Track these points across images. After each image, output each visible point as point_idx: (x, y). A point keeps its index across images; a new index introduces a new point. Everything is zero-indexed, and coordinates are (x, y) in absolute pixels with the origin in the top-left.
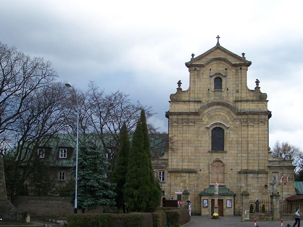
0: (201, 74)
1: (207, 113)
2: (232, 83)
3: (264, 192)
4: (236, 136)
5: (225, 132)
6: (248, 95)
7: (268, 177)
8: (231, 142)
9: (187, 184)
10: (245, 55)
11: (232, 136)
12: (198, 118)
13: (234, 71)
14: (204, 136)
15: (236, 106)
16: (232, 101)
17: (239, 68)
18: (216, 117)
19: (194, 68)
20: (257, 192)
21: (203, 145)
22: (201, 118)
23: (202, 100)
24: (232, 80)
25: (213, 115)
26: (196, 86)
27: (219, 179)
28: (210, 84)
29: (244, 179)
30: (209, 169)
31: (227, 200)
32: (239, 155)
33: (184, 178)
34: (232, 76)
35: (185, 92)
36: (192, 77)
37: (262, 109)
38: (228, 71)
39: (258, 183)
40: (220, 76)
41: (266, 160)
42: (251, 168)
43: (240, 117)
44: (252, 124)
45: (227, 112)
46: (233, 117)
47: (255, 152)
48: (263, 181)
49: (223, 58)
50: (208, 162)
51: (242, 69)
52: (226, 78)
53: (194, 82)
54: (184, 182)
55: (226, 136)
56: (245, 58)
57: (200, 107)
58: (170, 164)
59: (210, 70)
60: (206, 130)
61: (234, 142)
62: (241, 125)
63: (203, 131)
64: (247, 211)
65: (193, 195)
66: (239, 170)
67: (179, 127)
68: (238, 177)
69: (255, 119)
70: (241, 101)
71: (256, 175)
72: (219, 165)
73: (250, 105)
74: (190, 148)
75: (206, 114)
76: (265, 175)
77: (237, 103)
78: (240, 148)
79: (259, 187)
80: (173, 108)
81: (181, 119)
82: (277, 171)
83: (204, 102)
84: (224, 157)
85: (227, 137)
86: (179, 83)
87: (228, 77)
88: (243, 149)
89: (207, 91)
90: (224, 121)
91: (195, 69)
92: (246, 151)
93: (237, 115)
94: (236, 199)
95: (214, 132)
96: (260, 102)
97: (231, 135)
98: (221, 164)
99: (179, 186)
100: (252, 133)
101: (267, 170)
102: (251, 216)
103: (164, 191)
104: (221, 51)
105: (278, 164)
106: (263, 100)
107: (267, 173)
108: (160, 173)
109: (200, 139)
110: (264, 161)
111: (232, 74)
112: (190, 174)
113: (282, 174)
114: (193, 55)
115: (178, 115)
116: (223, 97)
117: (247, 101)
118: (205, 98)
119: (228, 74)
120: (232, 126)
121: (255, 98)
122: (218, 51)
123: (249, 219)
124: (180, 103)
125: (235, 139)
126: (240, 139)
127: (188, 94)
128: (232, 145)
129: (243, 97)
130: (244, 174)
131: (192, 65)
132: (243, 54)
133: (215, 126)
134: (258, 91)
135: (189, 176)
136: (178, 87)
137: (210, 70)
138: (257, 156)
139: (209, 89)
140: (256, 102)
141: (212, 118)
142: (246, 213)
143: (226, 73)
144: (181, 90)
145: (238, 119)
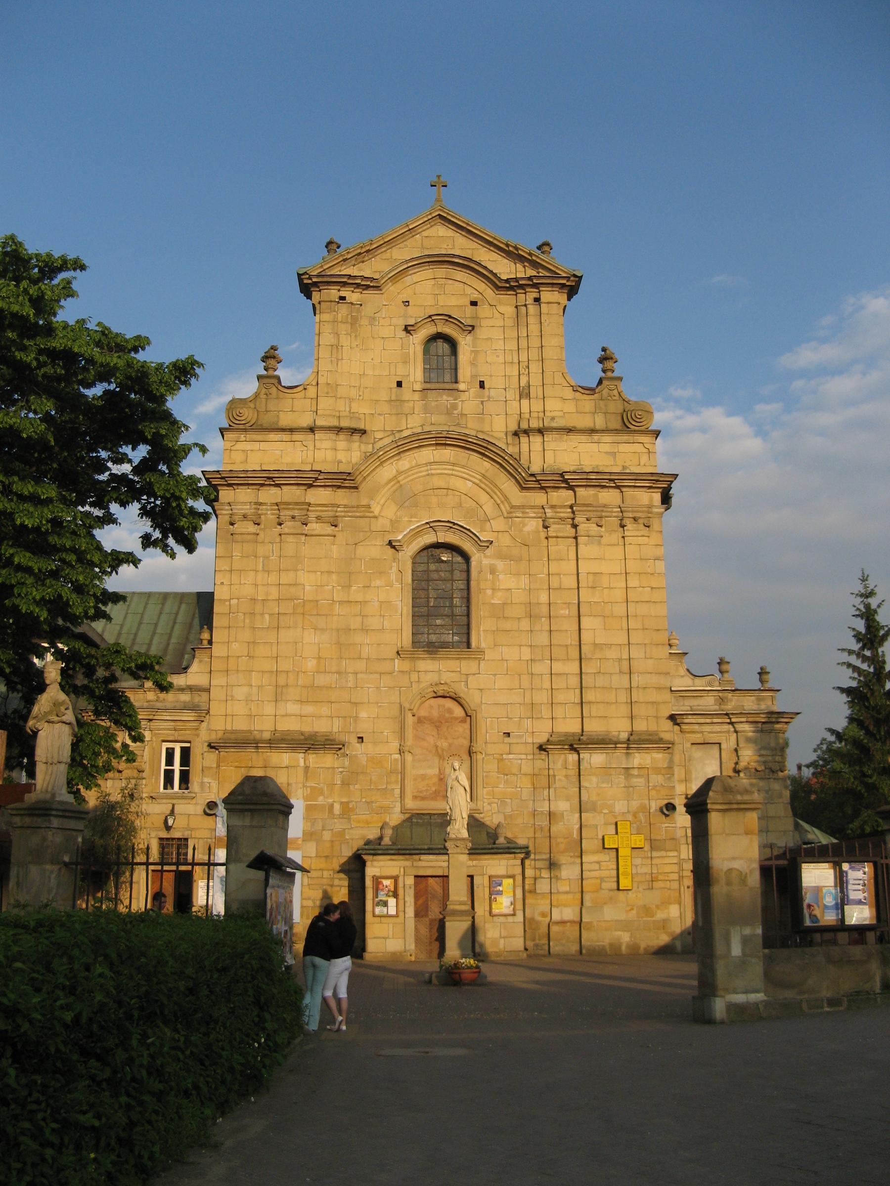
0: (364, 322)
1: (391, 480)
2: (501, 359)
3: (658, 837)
4: (524, 581)
6: (570, 407)
7: (676, 770)
8: (499, 612)
11: (506, 581)
13: (509, 310)
14: (378, 583)
16: (503, 435)
18: (434, 500)
21: (374, 623)
22: (364, 503)
23: (367, 428)
24: (500, 345)
25: (421, 488)
28: (406, 362)
29: (566, 776)
32: (541, 668)
35: (295, 390)
38: (483, 310)
40: (448, 330)
42: (594, 727)
43: (539, 498)
45: (484, 476)
46: (506, 498)
47: (613, 654)
48: (654, 787)
50: (395, 698)
51: (542, 300)
52: (475, 339)
53: (335, 351)
58: (216, 709)
62: (543, 535)
64: (747, 931)
65: (326, 857)
66: (542, 739)
67: (263, 542)
68: (536, 771)
69: (605, 506)
72: (447, 715)
74: (310, 637)
76: (658, 757)
77: (524, 439)
78: (544, 639)
79: (635, 815)
81: (272, 504)
82: (714, 738)
83: (379, 435)
84: (470, 678)
85: (482, 586)
87: (482, 333)
88: (558, 639)
91: (343, 298)
93: (523, 488)
94: (529, 872)
96: (625, 438)
97: (501, 577)
98: (458, 712)
100: (594, 567)
101: (666, 736)
103: (186, 839)
107: (668, 747)
108: (170, 754)
109: (359, 598)
110: (654, 696)
113: (736, 750)
116: (462, 414)
117: (570, 430)
118: (382, 418)
119: (484, 323)
120: (505, 540)
121: (599, 422)
123: (760, 997)
124: (273, 436)
125: (519, 597)
126: (544, 598)
128: (508, 625)
129: (553, 414)
130: (563, 756)
131: (325, 279)
133: (430, 538)
135: (307, 768)
138: (621, 672)
139: (399, 384)
140: (607, 438)
141: (416, 505)
142: (736, 950)
145: (533, 507)
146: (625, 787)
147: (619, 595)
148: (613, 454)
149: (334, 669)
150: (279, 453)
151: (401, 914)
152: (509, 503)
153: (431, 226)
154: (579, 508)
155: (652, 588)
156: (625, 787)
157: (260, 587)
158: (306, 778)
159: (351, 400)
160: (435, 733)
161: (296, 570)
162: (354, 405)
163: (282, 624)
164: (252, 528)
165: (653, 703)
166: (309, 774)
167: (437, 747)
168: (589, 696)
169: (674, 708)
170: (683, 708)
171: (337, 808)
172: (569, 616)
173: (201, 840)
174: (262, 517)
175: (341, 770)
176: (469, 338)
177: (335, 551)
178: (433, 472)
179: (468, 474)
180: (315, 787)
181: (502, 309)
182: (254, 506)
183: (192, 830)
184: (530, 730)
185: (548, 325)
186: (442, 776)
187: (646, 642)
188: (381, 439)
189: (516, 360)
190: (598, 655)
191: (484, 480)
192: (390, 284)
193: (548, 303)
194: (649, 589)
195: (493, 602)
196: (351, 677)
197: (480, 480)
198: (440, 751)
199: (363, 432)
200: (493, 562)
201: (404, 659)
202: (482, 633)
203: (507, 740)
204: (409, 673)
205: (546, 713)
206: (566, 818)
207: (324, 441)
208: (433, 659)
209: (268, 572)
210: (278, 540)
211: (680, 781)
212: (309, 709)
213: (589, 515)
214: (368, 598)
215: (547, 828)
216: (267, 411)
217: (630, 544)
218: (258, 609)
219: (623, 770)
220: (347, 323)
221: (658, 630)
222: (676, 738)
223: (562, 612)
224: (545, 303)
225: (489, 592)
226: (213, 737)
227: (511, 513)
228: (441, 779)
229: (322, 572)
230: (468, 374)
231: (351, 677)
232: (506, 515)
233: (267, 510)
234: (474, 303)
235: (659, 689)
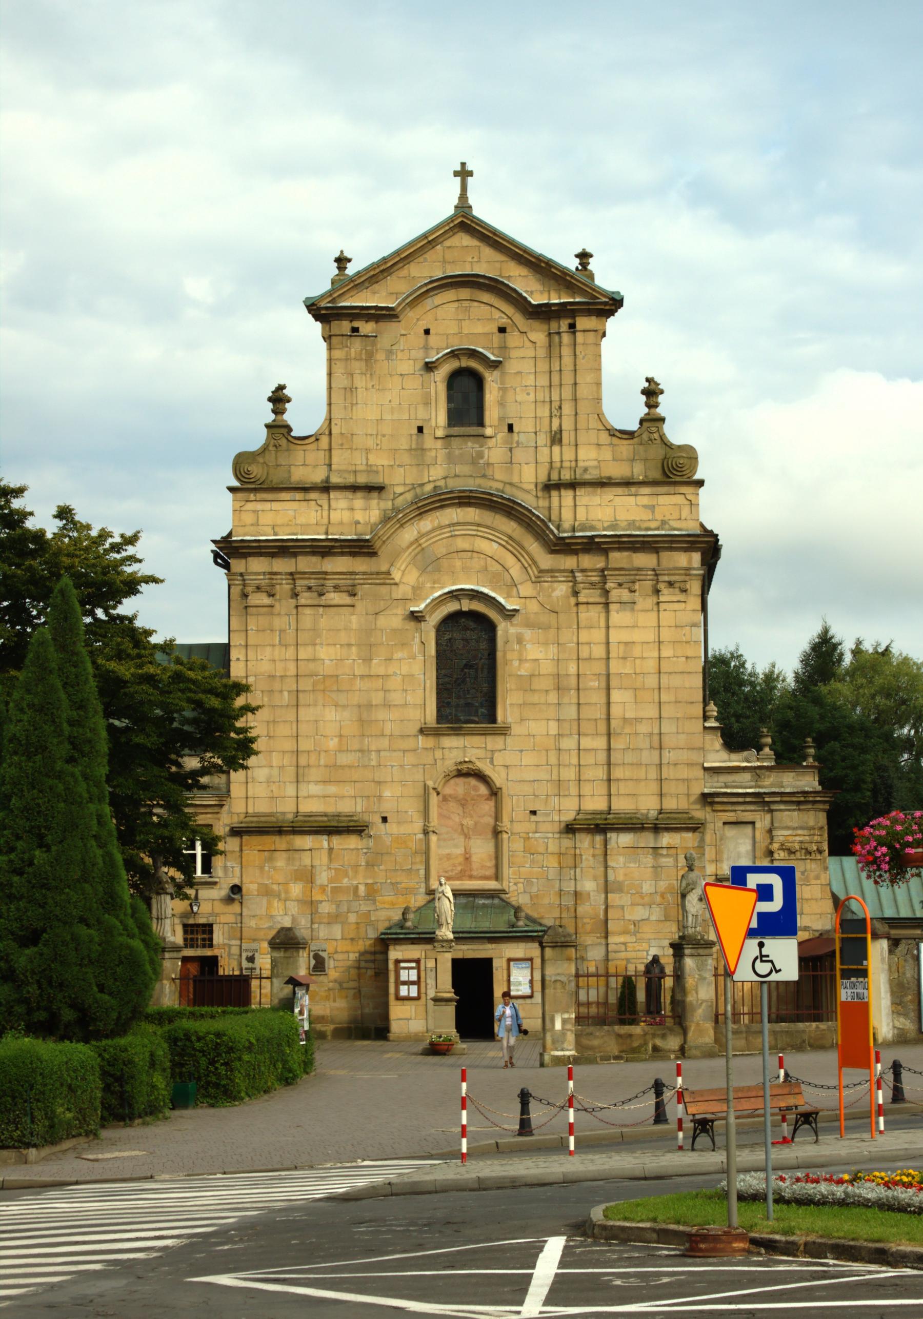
0: (380, 356)
1: (412, 544)
2: (532, 397)
4: (552, 650)
5: (500, 633)
6: (607, 454)
7: (707, 849)
8: (527, 684)
9: (323, 889)
10: (591, 260)
11: (533, 652)
12: (368, 570)
15: (550, 508)
16: (532, 487)
17: (564, 324)
18: (458, 563)
19: (345, 326)
20: (653, 918)
21: (396, 698)
22: (384, 568)
23: (387, 482)
24: (530, 380)
25: (443, 551)
26: (360, 412)
27: (474, 858)
28: (427, 403)
29: (594, 856)
30: (426, 813)
31: (509, 960)
32: (569, 743)
33: (306, 859)
34: (532, 362)
35: (307, 441)
36: (339, 369)
37: (674, 524)
38: (513, 338)
39: (656, 877)
42: (622, 805)
43: (569, 562)
44: (625, 595)
47: (643, 728)
49: (484, 277)
50: (419, 776)
51: (579, 326)
52: (503, 374)
53: (348, 394)
54: (308, 877)
56: (591, 276)
57: (377, 512)
59: (427, 332)
60: (412, 625)
61: (545, 683)
62: (573, 601)
63: (394, 631)
64: (566, 1016)
65: (352, 939)
66: (569, 816)
67: (279, 614)
68: (563, 850)
69: (639, 569)
70: (573, 485)
71: (647, 839)
72: (473, 793)
73: (618, 500)
74: (330, 714)
75: (408, 547)
76: (688, 839)
77: (554, 494)
78: (572, 712)
79: (663, 895)
80: (248, 518)
82: (748, 817)
83: (399, 490)
84: (496, 755)
85: (509, 656)
86: (279, 399)
87: (512, 366)
88: (586, 713)
89: (414, 437)
90: (494, 582)
92: (599, 722)
93: (553, 552)
95: (447, 637)
97: (528, 646)
98: (483, 790)
99: (283, 896)
102: (585, 1042)
103: (211, 925)
104: (475, 243)
105: (753, 784)
106: (678, 479)
109: (381, 671)
111: (531, 353)
112: (337, 841)
113: (770, 831)
114: (342, 261)
115: (273, 555)
116: (488, 464)
117: (603, 483)
118: (402, 470)
119: (514, 354)
120: (533, 606)
121: (638, 471)
122: (464, 240)
123: (573, 1053)
124: (284, 495)
125: (547, 668)
126: (572, 669)
127: (321, 454)
128: (535, 698)
132: (584, 256)
133: (453, 607)
134: (656, 436)
135: (331, 850)
136: (273, 416)
137: (427, 332)
139: (420, 429)
142: (558, 1026)
143: (504, 348)
144: (284, 431)
146: (653, 867)
147: (651, 665)
148: (652, 508)
149: (356, 747)
150: (291, 513)
151: (423, 996)
152: (537, 567)
153: (454, 234)
154: (611, 573)
155: (687, 658)
156: (653, 867)
157: (277, 663)
158: (330, 859)
159: (368, 451)
160: (460, 811)
161: (315, 645)
162: (371, 457)
163: (301, 702)
164: (267, 601)
165: (683, 780)
166: (333, 856)
167: (462, 825)
168: (617, 773)
169: (708, 785)
170: (715, 784)
171: (362, 888)
172: (599, 688)
173: (226, 926)
174: (278, 587)
175: (365, 851)
176: (496, 373)
177: (355, 621)
178: (457, 533)
180: (340, 869)
181: (534, 336)
182: (267, 577)
183: (217, 915)
184: (557, 808)
185: (583, 358)
186: (467, 856)
187: (679, 715)
188: (401, 494)
189: (547, 399)
190: (627, 731)
191: (510, 542)
192: (408, 309)
193: (584, 331)
194: (684, 659)
195: (519, 673)
196: (373, 755)
197: (507, 542)
198: (466, 830)
199: (380, 489)
200: (520, 630)
201: (427, 735)
202: (508, 706)
203: (533, 818)
204: (433, 749)
205: (573, 791)
206: (592, 898)
207: (340, 501)
209: (286, 646)
210: (294, 611)
211: (711, 861)
212: (332, 789)
213: (621, 579)
214: (390, 672)
215: (573, 910)
216: (277, 466)
218: (277, 686)
219: (651, 850)
220: (361, 359)
221: (692, 703)
222: (707, 816)
223: (592, 684)
225: (516, 663)
226: (235, 821)
227: (539, 577)
228: (467, 859)
229: (341, 645)
231: (373, 755)
232: (534, 579)
233: (282, 579)
235: (690, 765)
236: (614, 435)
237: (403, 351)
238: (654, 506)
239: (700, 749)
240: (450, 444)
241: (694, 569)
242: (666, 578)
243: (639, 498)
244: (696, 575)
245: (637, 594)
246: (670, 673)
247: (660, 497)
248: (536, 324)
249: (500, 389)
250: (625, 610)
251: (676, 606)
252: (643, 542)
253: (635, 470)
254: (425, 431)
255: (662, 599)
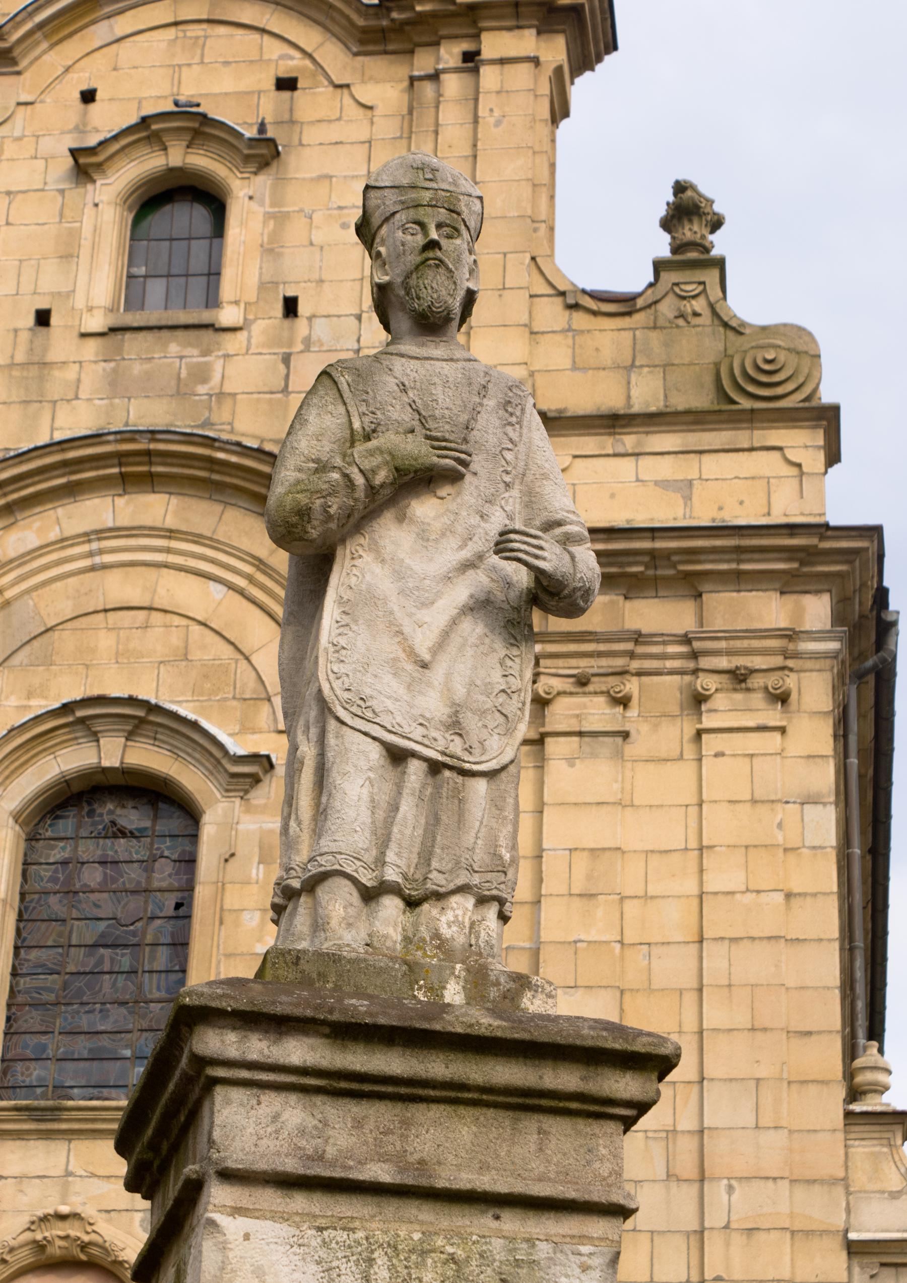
5: (209, 830)
41: (808, 1233)
55: (221, 887)
85: (231, 900)
89: (24, 336)
95: (59, 853)
116: (221, 395)
119: (311, 135)
134: (699, 305)
137: (88, 97)
139: (43, 318)
141: (47, 661)
148: (686, 488)
155: (789, 896)
176: (263, 182)
178: (108, 558)
179: (213, 561)
181: (366, 93)
185: (498, 123)
187: (762, 1072)
193: (502, 61)
194: (779, 898)
197: (250, 579)
208: (48, 1135)
217: (716, 755)
221: (809, 1033)
224: (493, 62)
230: (253, 279)
234: (286, 84)
236: (574, 307)
237: (19, 139)
238: (690, 482)
239: (833, 1182)
240: (119, 350)
241: (811, 636)
242: (723, 663)
243: (645, 461)
244: (816, 656)
245: (633, 713)
246: (734, 940)
247: (706, 458)
248: (376, 65)
249: (268, 216)
250: (594, 755)
251: (755, 742)
252: (653, 554)
253: (634, 393)
254: (54, 320)
255: (708, 721)
